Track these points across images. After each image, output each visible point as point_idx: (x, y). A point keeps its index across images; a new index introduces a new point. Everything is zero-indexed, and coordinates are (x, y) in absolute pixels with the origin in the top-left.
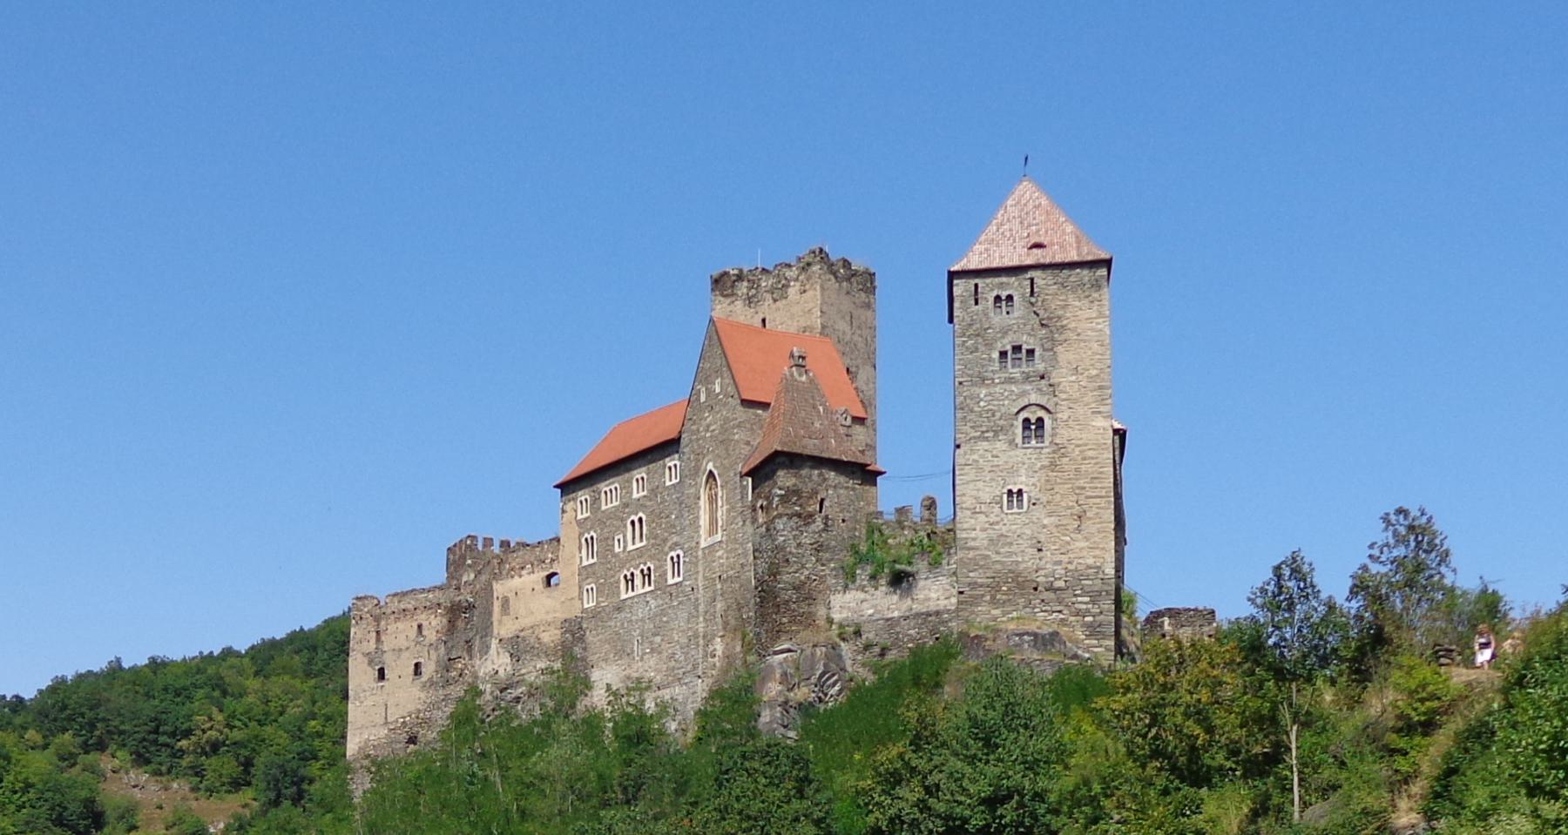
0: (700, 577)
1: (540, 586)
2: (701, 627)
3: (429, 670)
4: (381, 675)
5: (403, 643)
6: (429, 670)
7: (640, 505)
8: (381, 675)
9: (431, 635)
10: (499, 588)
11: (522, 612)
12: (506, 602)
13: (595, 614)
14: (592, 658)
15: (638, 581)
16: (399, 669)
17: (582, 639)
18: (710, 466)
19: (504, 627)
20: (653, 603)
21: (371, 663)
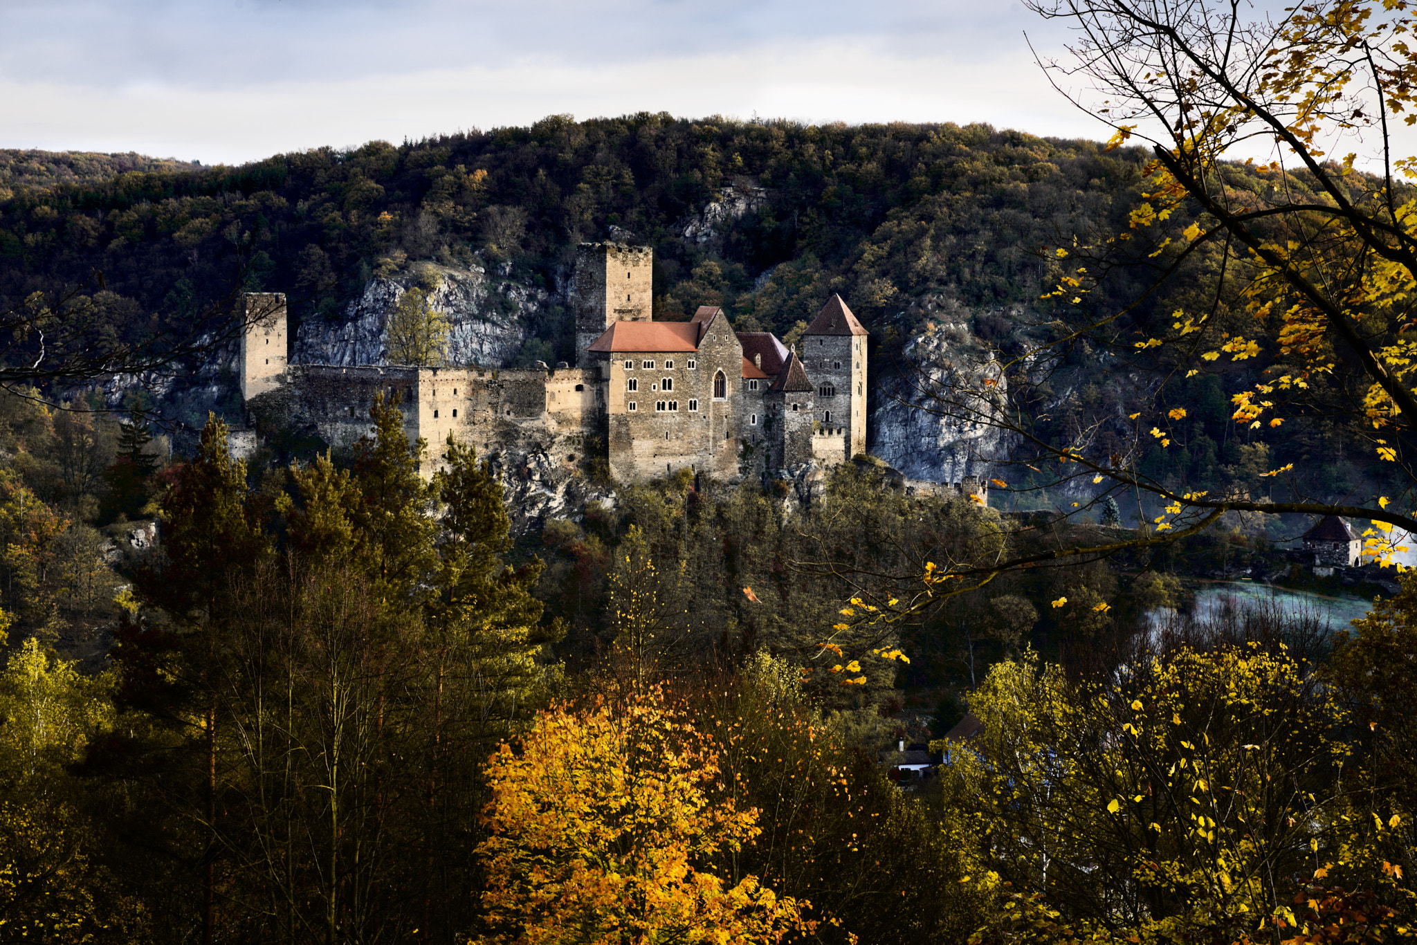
0: (711, 414)
1: (573, 390)
2: (711, 433)
3: (460, 414)
4: (436, 414)
5: (447, 399)
6: (460, 414)
7: (668, 374)
8: (436, 414)
9: (461, 395)
10: (549, 387)
11: (562, 401)
12: (553, 394)
13: (636, 416)
14: (632, 435)
15: (667, 406)
16: (445, 412)
17: (626, 425)
18: (720, 369)
19: (552, 406)
20: (678, 418)
21: (431, 407)
